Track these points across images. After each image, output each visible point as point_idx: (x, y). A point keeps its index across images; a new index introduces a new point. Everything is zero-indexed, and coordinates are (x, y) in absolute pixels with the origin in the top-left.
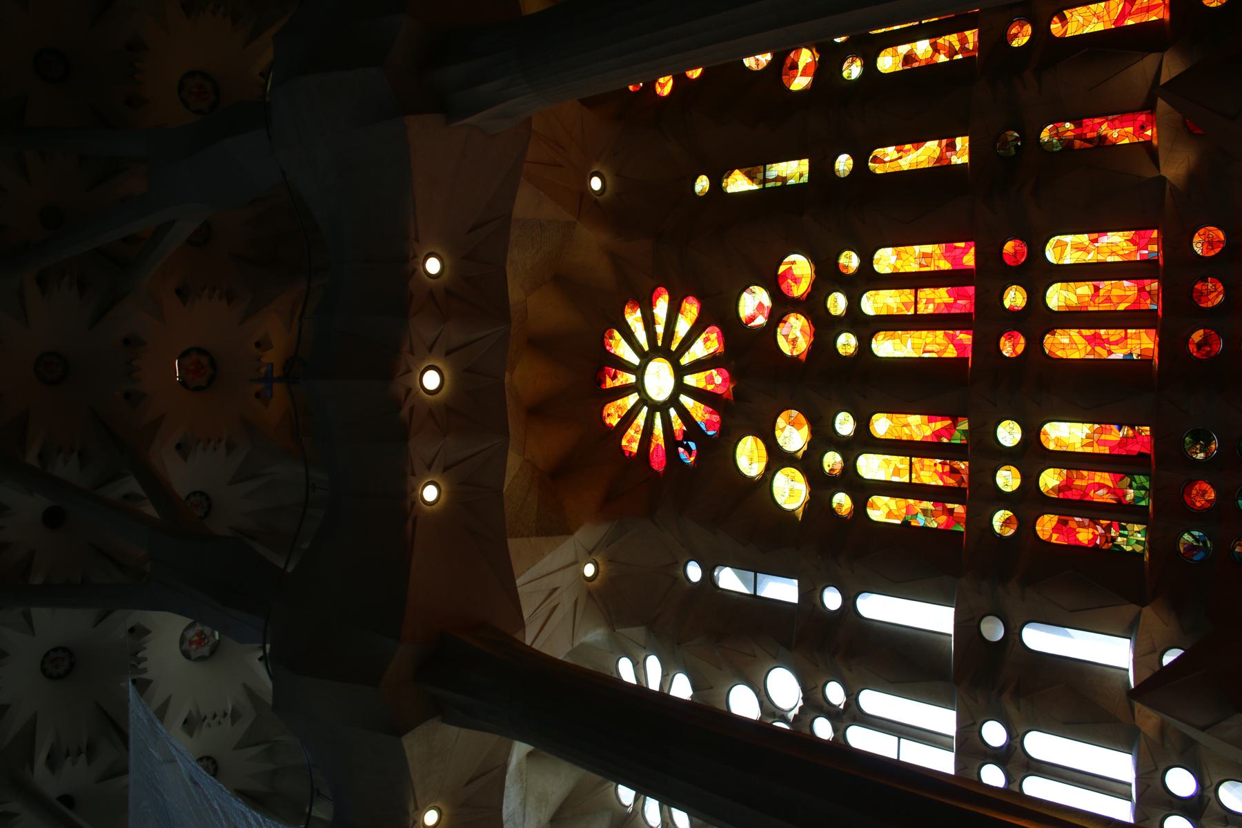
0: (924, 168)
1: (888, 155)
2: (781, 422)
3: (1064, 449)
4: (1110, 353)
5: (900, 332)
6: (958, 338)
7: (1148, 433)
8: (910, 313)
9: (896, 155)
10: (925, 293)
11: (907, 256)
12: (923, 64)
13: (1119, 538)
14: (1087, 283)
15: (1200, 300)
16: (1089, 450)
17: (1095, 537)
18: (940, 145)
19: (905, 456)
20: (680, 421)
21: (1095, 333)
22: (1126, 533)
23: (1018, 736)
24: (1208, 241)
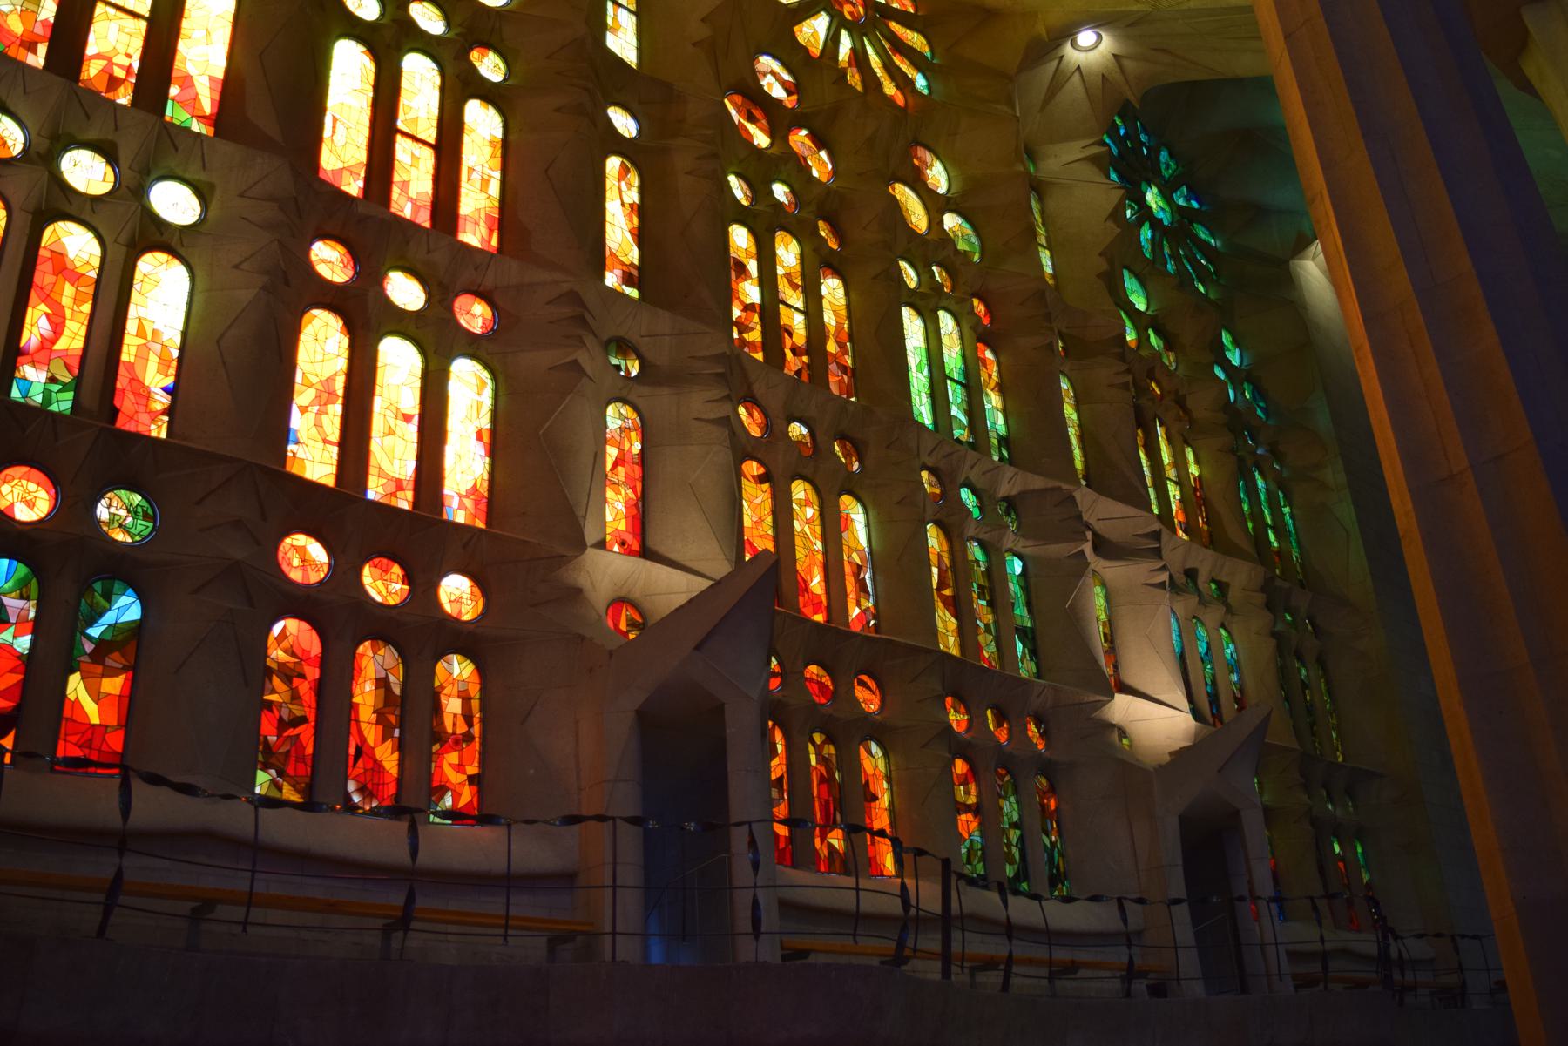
1: (629, 189)
3: (137, 286)
4: (303, 410)
7: (154, 434)
9: (628, 200)
10: (427, 158)
12: (734, 285)
14: (418, 407)
15: (375, 567)
16: (131, 326)
18: (632, 264)
21: (339, 397)
24: (461, 598)
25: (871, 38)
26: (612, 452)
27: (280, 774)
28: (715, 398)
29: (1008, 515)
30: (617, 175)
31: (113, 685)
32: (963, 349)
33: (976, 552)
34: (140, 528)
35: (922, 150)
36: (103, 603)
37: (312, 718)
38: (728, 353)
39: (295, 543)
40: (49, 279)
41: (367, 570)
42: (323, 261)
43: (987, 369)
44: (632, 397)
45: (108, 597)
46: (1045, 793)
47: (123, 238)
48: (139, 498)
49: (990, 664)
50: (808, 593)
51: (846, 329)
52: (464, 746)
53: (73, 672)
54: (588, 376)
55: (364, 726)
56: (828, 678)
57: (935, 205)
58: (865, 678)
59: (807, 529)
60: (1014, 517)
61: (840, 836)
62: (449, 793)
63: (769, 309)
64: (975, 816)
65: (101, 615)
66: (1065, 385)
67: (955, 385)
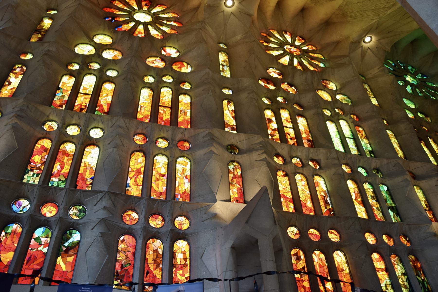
1: (231, 107)
2: (116, 53)
3: (85, 154)
5: (152, 99)
6: (146, 119)
9: (230, 109)
10: (168, 111)
11: (186, 107)
12: (268, 125)
13: (33, 173)
14: (167, 172)
15: (153, 217)
16: (82, 164)
17: (34, 162)
18: (234, 125)
22: (35, 176)
25: (303, 58)
26: (231, 175)
27: (121, 281)
28: (261, 153)
29: (378, 173)
30: (227, 104)
31: (70, 259)
32: (351, 129)
33: (366, 186)
34: (81, 215)
36: (69, 236)
38: (263, 140)
39: (128, 214)
40: (61, 156)
42: (137, 140)
43: (360, 133)
45: (71, 234)
46: (414, 261)
47: (80, 142)
48: (82, 207)
50: (306, 207)
51: (308, 130)
52: (184, 268)
53: (59, 256)
54: (215, 153)
55: (149, 264)
56: (318, 232)
57: (333, 93)
61: (331, 285)
63: (281, 128)
64: (386, 272)
65: (69, 239)
66: (389, 132)
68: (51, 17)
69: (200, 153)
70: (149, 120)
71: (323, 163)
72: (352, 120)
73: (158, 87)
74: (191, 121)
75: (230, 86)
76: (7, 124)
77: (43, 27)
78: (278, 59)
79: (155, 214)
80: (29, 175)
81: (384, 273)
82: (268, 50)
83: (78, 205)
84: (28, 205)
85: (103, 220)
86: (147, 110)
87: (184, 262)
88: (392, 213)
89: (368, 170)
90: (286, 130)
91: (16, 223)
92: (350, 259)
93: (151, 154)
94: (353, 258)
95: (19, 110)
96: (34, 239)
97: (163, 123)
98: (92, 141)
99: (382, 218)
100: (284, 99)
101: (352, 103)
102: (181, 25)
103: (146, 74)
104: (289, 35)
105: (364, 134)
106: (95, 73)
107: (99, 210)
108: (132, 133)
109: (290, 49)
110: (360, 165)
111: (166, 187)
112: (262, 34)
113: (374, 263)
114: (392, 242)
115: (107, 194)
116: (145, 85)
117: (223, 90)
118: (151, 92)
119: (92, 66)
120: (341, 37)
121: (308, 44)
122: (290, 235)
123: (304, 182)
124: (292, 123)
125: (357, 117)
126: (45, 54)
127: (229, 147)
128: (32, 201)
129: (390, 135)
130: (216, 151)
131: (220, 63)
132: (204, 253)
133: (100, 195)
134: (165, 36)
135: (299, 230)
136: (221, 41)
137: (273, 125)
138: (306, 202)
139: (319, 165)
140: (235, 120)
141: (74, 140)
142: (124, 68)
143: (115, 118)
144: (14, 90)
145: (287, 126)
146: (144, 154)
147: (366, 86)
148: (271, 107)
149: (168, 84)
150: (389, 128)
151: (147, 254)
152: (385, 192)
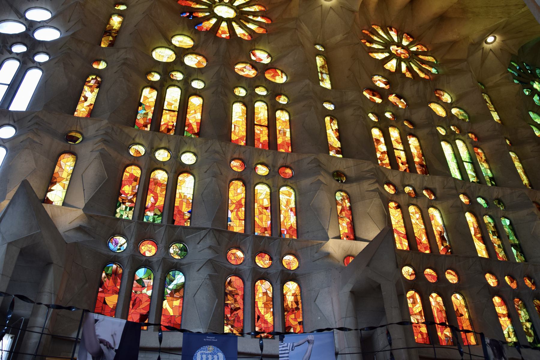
0: (327, 139)
2: (200, 58)
3: (178, 184)
4: (232, 211)
5: (245, 116)
7: (186, 225)
8: (255, 122)
10: (265, 131)
11: (285, 125)
13: (125, 206)
14: (270, 204)
17: (126, 194)
18: (339, 148)
19: (179, 109)
20: (203, 16)
22: (128, 210)
23: (4, 143)
26: (339, 208)
27: (232, 326)
28: (372, 183)
29: (499, 204)
31: (177, 303)
32: (468, 151)
33: (487, 219)
34: (183, 254)
35: (439, 91)
36: (173, 278)
37: (242, 307)
39: (232, 252)
40: (153, 186)
41: (257, 258)
42: (235, 166)
43: (479, 155)
44: (344, 189)
45: (174, 276)
47: (173, 170)
48: (182, 245)
49: (503, 259)
50: (421, 244)
51: (421, 153)
54: (323, 183)
55: (260, 308)
56: (434, 273)
57: (447, 107)
58: (449, 271)
59: (417, 222)
60: (502, 204)
61: (449, 331)
62: (292, 329)
63: (390, 151)
66: (512, 155)
67: (467, 163)
68: (120, 14)
69: (306, 182)
70: (245, 142)
71: (438, 192)
72: (470, 140)
73: (252, 101)
74: (291, 143)
75: (332, 100)
76: (93, 150)
77: (113, 26)
78: (383, 64)
79: (261, 252)
80: (121, 209)
81: (506, 319)
82: (372, 52)
83: (178, 243)
84: (125, 243)
85: (210, 261)
86: (241, 129)
87: (296, 306)
88: (515, 251)
89: (489, 201)
90: (397, 153)
91: (116, 264)
92: (469, 303)
93: (252, 183)
94: (473, 303)
95: (104, 134)
96: (136, 281)
97: (260, 146)
98: (185, 168)
99: (504, 257)
100: (393, 115)
101: (469, 118)
102: (270, 22)
103: (237, 85)
104: (395, 32)
105: (484, 158)
106: (179, 84)
107: (204, 249)
108: (229, 158)
109: (397, 50)
110: (480, 194)
111: (270, 222)
112: (364, 31)
113: (496, 307)
114: (516, 284)
115: (211, 231)
116: (236, 100)
117: (324, 105)
118: (244, 108)
119: (174, 75)
120: (458, 37)
121: (418, 44)
122: (405, 276)
123: (418, 216)
124: (402, 144)
125: (476, 136)
126: (124, 64)
127: (335, 173)
128: (129, 238)
129: (513, 158)
130: (324, 181)
131: (319, 71)
132: (317, 296)
133: (203, 233)
134: (253, 37)
135: (414, 270)
136: (317, 42)
137: (382, 148)
138: (421, 238)
139: (434, 195)
140: (340, 141)
141: (165, 168)
142: (212, 78)
143: (209, 141)
144: (92, 107)
145: (398, 148)
146: (243, 183)
147: (486, 97)
148: (378, 125)
149: (263, 97)
150: (513, 150)
151: (257, 297)
152: (507, 227)
